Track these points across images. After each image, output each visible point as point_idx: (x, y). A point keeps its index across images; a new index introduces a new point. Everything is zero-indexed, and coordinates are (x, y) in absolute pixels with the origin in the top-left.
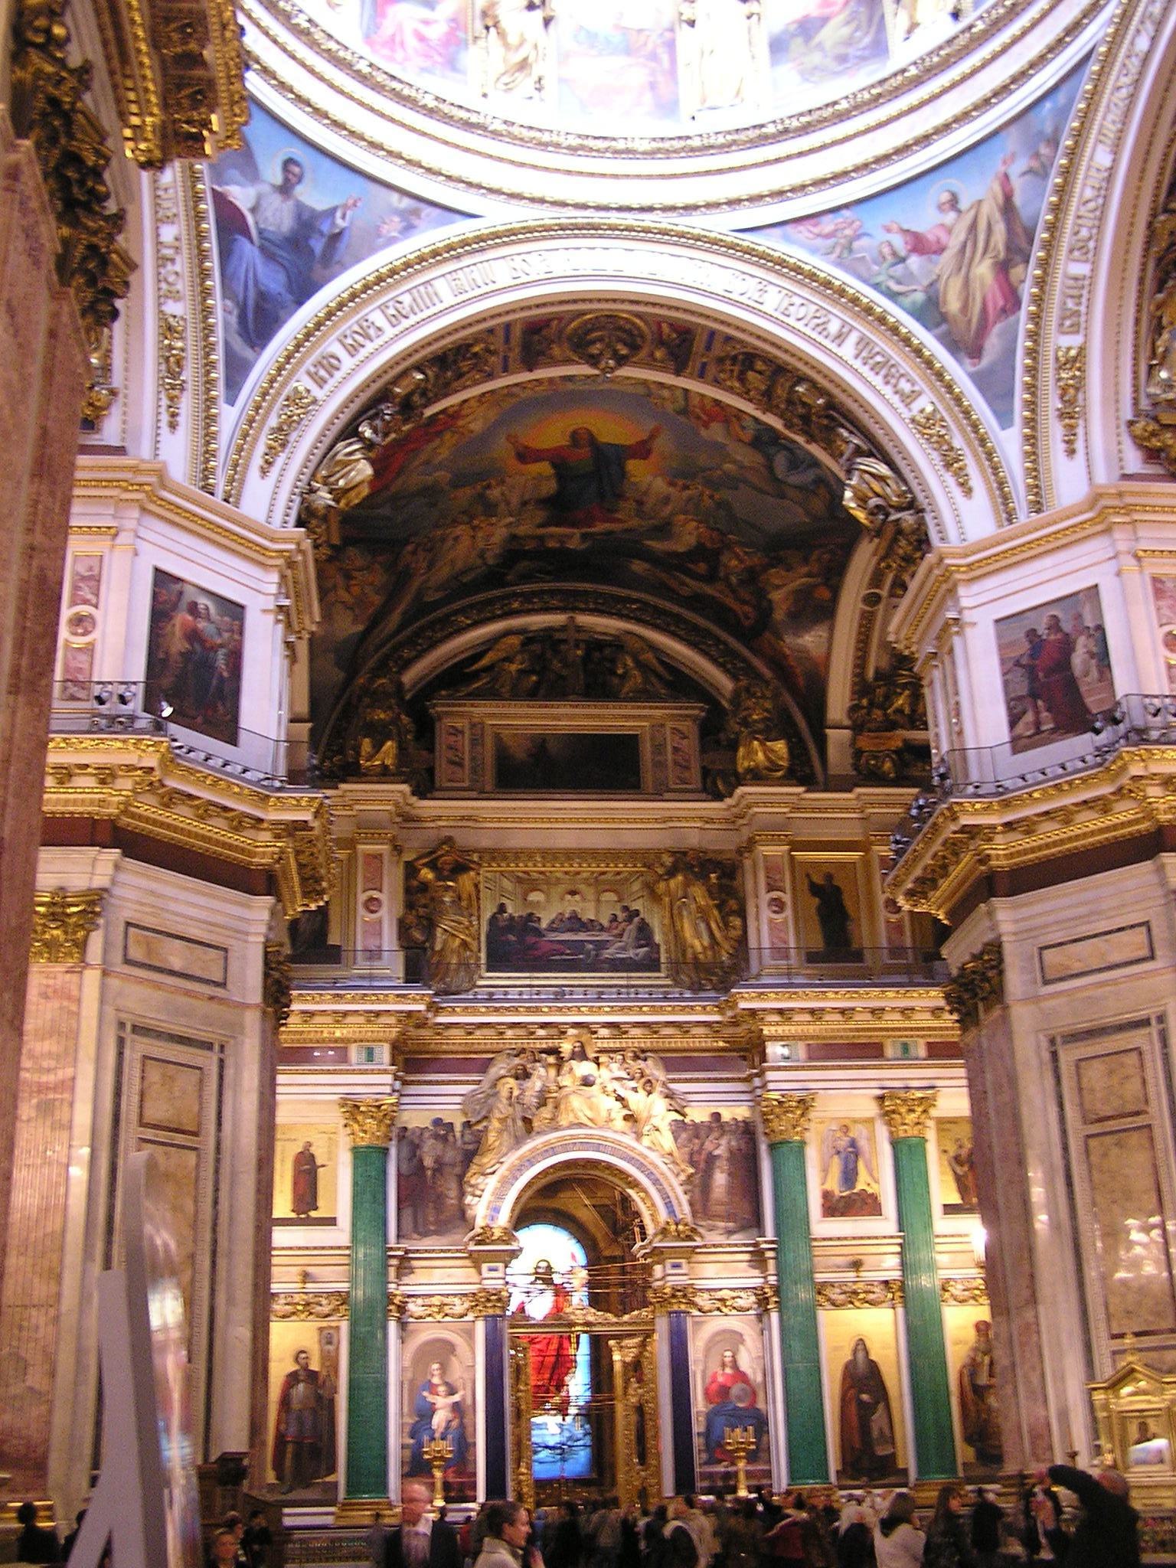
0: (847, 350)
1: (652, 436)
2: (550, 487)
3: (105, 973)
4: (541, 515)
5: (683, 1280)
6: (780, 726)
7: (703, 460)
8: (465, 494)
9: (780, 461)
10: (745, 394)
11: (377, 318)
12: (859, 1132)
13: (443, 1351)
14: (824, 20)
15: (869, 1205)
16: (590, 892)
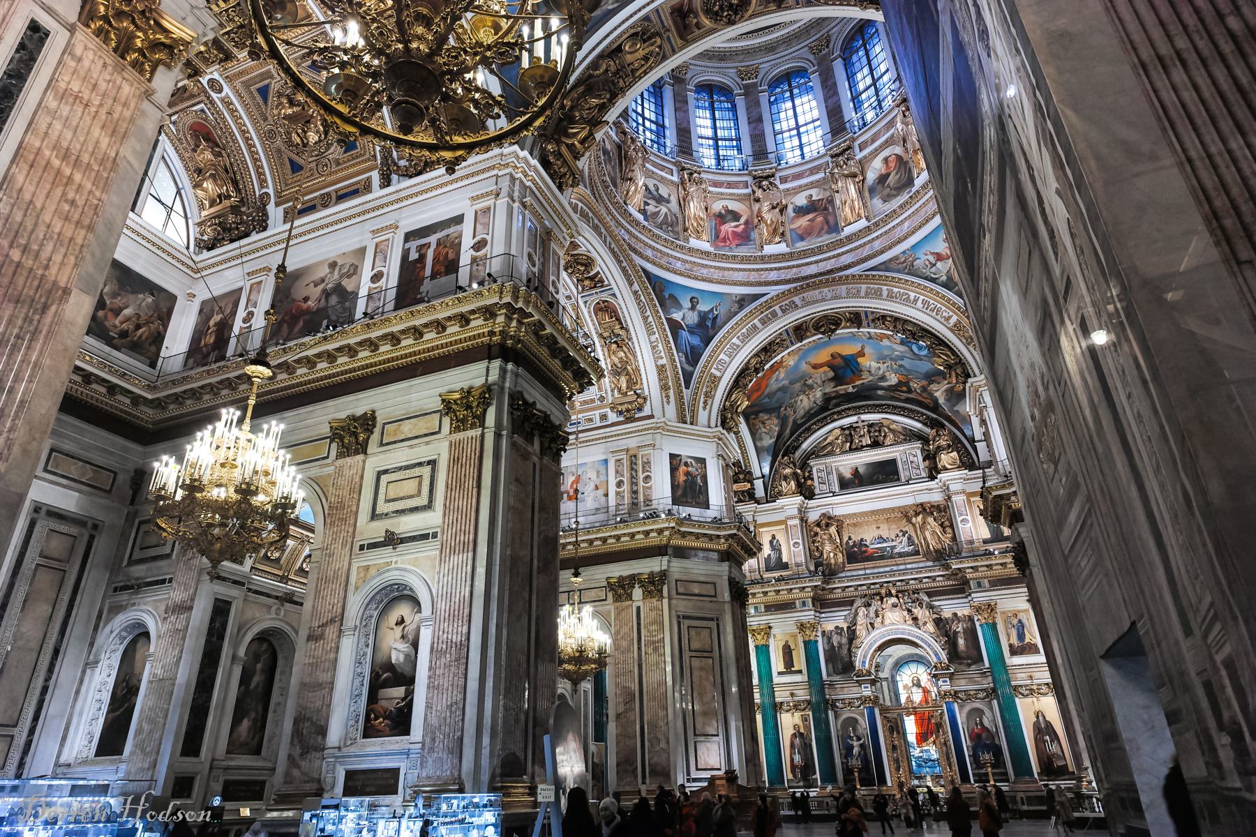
0: (919, 304)
1: (863, 348)
2: (831, 374)
3: (670, 599)
4: (832, 384)
5: (948, 688)
6: (956, 444)
7: (886, 352)
8: (798, 386)
9: (914, 348)
10: (888, 329)
11: (738, 342)
12: (1022, 616)
13: (853, 722)
14: (888, 175)
15: (1032, 649)
16: (884, 527)
